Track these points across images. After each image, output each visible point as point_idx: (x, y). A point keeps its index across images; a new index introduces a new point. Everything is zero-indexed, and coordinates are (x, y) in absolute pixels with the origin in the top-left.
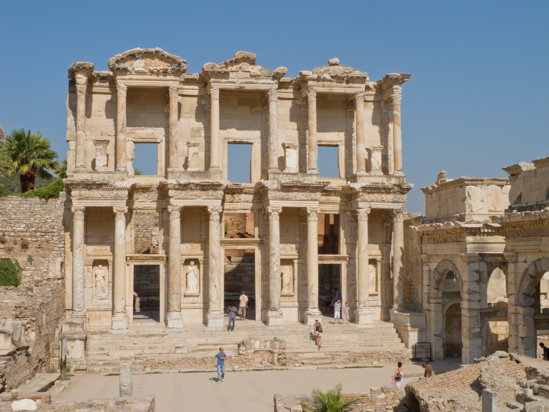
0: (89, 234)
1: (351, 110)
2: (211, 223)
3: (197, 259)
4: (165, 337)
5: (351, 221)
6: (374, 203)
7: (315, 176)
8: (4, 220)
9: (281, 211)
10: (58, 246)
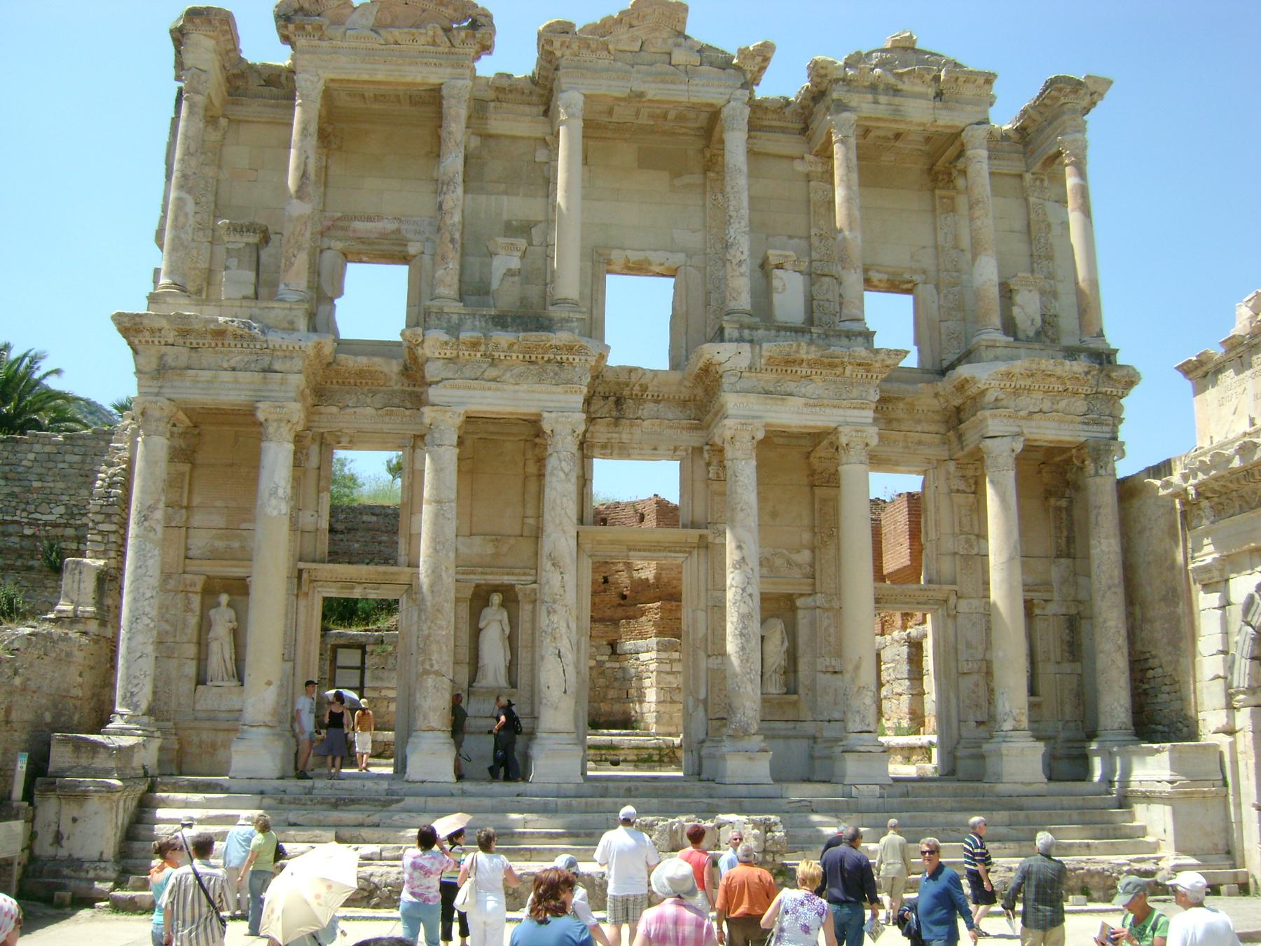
0: (196, 501)
1: (944, 193)
2: (552, 463)
3: (513, 586)
4: (394, 807)
5: (958, 491)
6: (1033, 424)
7: (860, 340)
8: (13, 495)
9: (760, 435)
10: (101, 527)
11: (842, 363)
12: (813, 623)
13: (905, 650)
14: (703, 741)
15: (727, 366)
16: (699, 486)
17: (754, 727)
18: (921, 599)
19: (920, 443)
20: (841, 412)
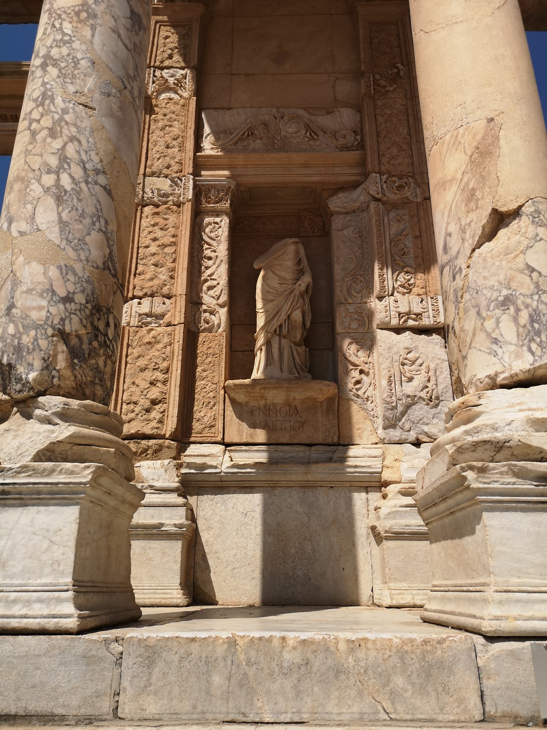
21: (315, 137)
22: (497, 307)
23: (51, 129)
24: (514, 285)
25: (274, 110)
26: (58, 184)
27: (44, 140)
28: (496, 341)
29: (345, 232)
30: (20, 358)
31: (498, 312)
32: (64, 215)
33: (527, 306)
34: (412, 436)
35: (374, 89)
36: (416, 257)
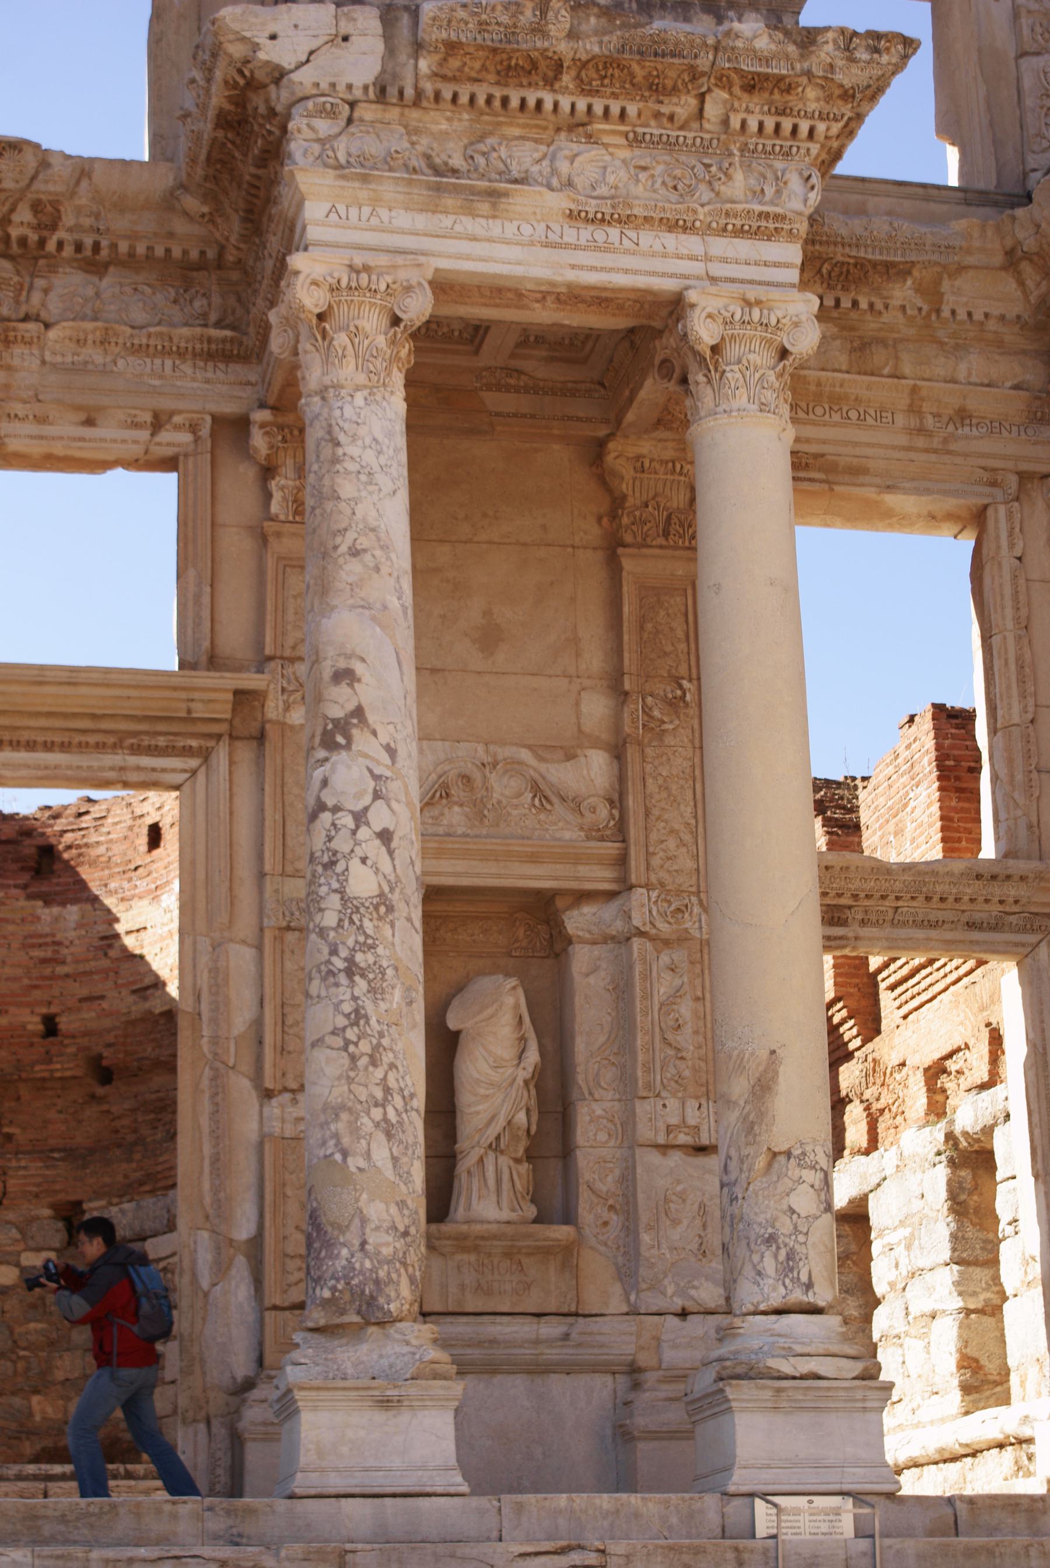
11: (695, 75)
12: (622, 990)
13: (942, 1173)
14: (249, 1384)
15: (305, 78)
16: (236, 545)
17: (400, 1297)
18: (982, 913)
19: (962, 416)
20: (692, 243)
21: (548, 807)
22: (763, 1243)
23: (371, 1056)
24: (777, 1225)
25: (481, 748)
26: (386, 1119)
27: (366, 1069)
28: (759, 1273)
29: (592, 980)
30: (380, 1290)
31: (763, 1248)
32: (394, 1150)
33: (786, 1245)
34: (678, 1303)
35: (644, 725)
36: (696, 1032)
